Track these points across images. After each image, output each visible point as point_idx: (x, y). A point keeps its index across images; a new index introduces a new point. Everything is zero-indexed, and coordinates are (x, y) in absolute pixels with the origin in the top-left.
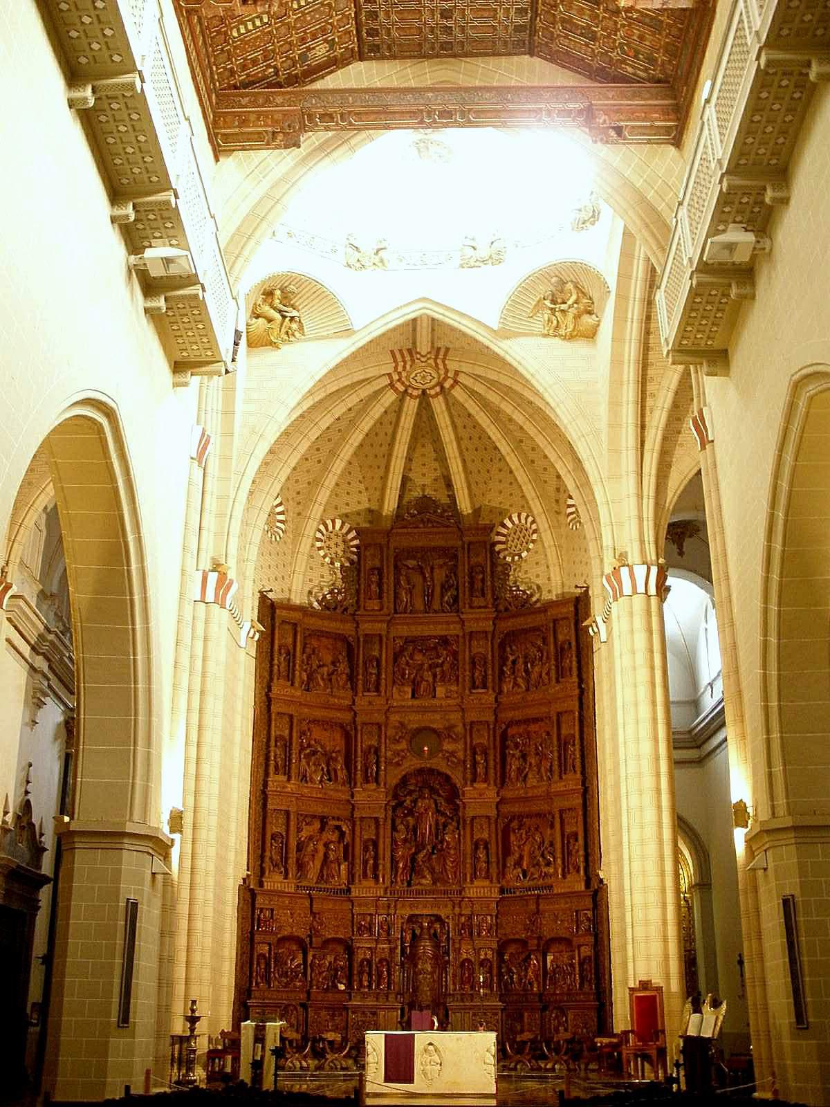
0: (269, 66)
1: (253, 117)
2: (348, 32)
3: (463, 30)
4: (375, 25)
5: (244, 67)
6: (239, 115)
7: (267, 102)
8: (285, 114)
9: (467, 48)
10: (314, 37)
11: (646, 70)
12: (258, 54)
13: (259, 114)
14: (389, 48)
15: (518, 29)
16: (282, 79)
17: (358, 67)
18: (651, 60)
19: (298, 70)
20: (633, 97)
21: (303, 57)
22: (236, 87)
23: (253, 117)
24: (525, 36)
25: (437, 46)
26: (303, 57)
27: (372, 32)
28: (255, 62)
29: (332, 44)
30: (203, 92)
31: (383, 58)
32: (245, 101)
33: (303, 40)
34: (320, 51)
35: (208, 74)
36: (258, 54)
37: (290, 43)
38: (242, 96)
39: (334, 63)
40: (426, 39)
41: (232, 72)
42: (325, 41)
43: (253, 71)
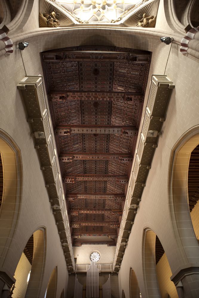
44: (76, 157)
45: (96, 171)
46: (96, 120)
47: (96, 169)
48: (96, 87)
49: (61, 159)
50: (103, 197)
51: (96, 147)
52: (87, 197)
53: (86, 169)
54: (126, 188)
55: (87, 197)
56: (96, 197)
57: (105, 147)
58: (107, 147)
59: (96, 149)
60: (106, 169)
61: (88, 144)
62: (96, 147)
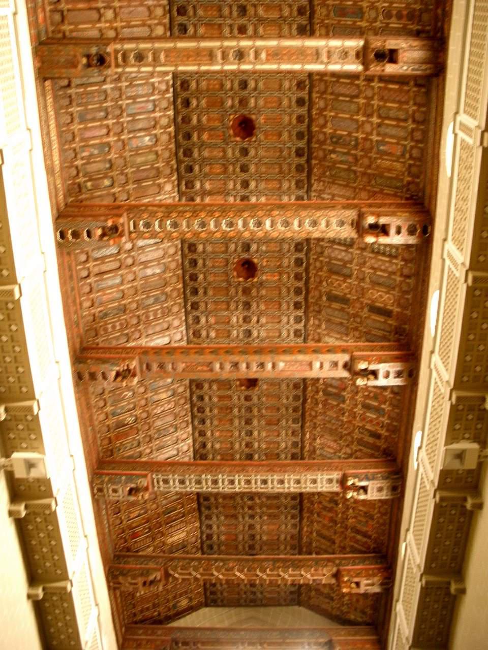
0: (155, 611)
1: (144, 642)
2: (198, 593)
3: (262, 593)
4: (214, 589)
5: (142, 611)
6: (137, 640)
7: (153, 633)
8: (163, 641)
9: (264, 602)
10: (181, 595)
11: (362, 617)
12: (150, 605)
13: (148, 641)
14: (222, 601)
15: (291, 593)
16: (162, 617)
17: (205, 611)
18: (363, 612)
19: (171, 613)
20: (354, 635)
21: (175, 606)
22: (136, 623)
23: (144, 642)
24: (295, 596)
25: (248, 601)
26: (175, 606)
27: (212, 593)
28: (148, 609)
29: (191, 599)
30: (118, 628)
31: (218, 606)
32: (141, 631)
33: (175, 597)
34: (184, 603)
35: (122, 617)
36: (150, 605)
37: (168, 600)
38: (140, 628)
39: (191, 609)
40: (242, 598)
41: (135, 615)
42: (187, 597)
43: (147, 614)
44: (341, 364)
45: (244, 169)
46: (250, 433)
47: (246, 184)
48: (251, 527)
49: (405, 374)
50: (187, 56)
51: (246, 320)
52: (301, 55)
53: (299, 168)
54: (52, 123)
55: (301, 55)
56: (241, 55)
57: (203, 320)
58: (197, 320)
59: (247, 306)
60: (188, 153)
61: (284, 334)
62: (246, 320)
